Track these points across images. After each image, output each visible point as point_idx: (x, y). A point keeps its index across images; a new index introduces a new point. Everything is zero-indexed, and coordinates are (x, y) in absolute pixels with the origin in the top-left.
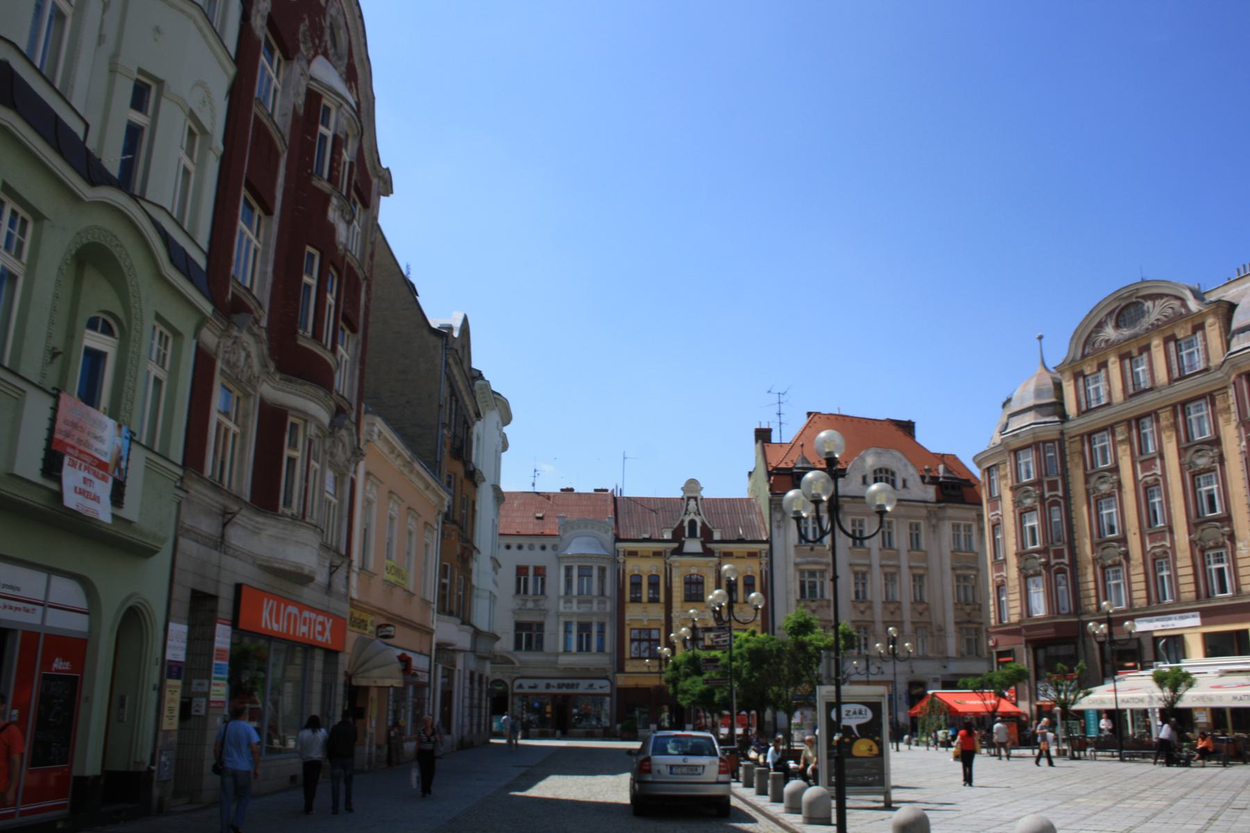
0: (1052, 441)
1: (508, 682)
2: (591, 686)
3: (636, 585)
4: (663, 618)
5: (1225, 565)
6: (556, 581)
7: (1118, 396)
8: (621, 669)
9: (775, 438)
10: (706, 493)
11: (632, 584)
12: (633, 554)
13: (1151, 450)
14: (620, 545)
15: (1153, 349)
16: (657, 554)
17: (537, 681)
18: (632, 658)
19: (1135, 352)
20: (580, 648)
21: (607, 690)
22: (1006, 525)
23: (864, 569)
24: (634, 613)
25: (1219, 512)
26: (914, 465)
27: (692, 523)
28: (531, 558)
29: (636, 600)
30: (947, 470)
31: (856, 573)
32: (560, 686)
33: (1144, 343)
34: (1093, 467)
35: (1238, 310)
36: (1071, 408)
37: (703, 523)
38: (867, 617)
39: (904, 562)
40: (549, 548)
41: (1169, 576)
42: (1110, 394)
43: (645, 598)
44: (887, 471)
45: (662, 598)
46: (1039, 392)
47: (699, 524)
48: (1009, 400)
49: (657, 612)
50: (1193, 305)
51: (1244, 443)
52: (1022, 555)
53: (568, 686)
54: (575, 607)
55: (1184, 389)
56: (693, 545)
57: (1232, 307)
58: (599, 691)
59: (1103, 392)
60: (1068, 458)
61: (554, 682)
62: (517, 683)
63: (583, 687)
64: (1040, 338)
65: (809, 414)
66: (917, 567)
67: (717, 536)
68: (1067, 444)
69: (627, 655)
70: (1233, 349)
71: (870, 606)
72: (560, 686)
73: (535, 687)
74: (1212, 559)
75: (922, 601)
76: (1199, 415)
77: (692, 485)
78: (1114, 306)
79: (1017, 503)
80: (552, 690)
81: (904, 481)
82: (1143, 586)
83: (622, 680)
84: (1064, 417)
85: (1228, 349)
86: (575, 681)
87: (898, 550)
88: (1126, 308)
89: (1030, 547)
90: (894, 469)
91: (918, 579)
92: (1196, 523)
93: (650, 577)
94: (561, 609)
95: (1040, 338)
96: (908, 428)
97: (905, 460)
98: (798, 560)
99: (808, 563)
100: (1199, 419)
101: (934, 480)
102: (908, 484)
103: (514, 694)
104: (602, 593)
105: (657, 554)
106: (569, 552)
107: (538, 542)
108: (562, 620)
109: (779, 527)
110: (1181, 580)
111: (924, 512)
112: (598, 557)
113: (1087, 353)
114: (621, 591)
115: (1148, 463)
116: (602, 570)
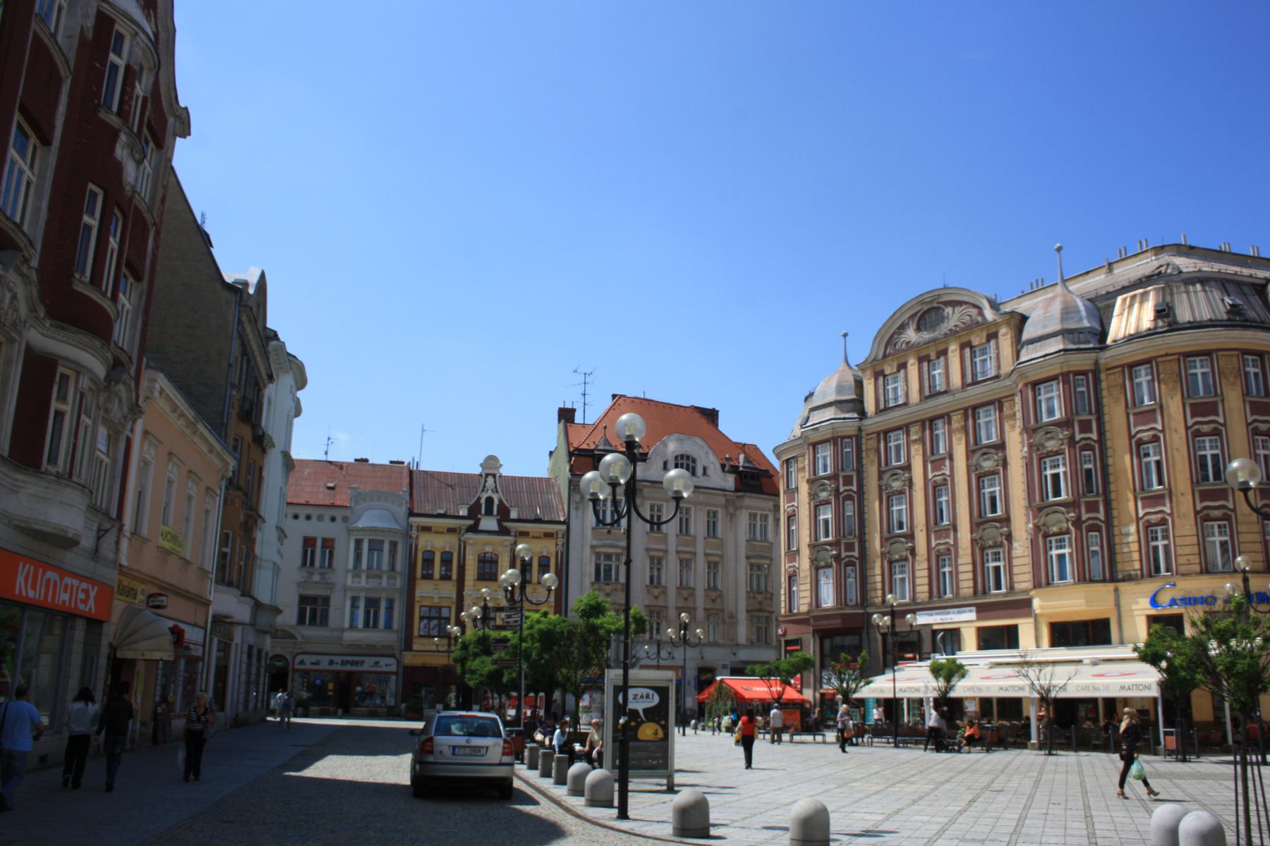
0: (850, 437)
1: (289, 657)
2: (377, 663)
3: (428, 562)
4: (454, 596)
5: (1001, 564)
6: (345, 554)
7: (915, 396)
8: (408, 646)
9: (578, 419)
10: (505, 471)
11: (424, 560)
12: (427, 529)
13: (942, 451)
14: (413, 519)
15: (950, 354)
16: (451, 530)
17: (320, 658)
18: (420, 636)
19: (933, 356)
20: (367, 625)
21: (393, 668)
22: (801, 515)
23: (660, 554)
24: (424, 590)
25: (999, 513)
27: (490, 501)
28: (319, 530)
29: (428, 577)
30: (747, 460)
31: (652, 558)
32: (344, 663)
33: (942, 347)
34: (887, 464)
35: (1029, 322)
36: (870, 406)
37: (500, 501)
38: (661, 602)
39: (700, 549)
40: (339, 519)
41: (951, 572)
42: (907, 394)
43: (437, 575)
44: (688, 457)
45: (454, 576)
46: (840, 388)
47: (496, 502)
48: (811, 395)
49: (449, 590)
50: (989, 315)
51: (1026, 449)
52: (815, 547)
53: (352, 663)
54: (363, 582)
55: (976, 394)
56: (489, 523)
57: (1023, 319)
58: (385, 669)
59: (900, 392)
60: (864, 454)
61: (338, 659)
62: (298, 659)
63: (368, 664)
64: (845, 335)
65: (614, 396)
67: (514, 515)
68: (864, 441)
69: (416, 633)
70: (1022, 359)
71: (664, 592)
72: (344, 663)
73: (317, 663)
75: (715, 588)
76: (988, 418)
77: (491, 462)
78: (912, 312)
79: (813, 496)
80: (335, 667)
81: (705, 469)
82: (926, 580)
83: (409, 659)
84: (863, 414)
86: (360, 659)
87: (695, 537)
88: (928, 312)
89: (823, 540)
90: (696, 456)
91: (713, 566)
92: (978, 523)
93: (443, 553)
94: (349, 583)
95: (845, 335)
96: (711, 416)
97: (706, 447)
98: (595, 543)
99: (604, 546)
100: (988, 423)
101: (734, 470)
102: (709, 472)
103: (295, 671)
104: (393, 567)
105: (451, 530)
106: (360, 525)
107: (328, 513)
108: (349, 594)
109: (577, 508)
110: (961, 577)
111: (723, 500)
112: (390, 531)
113: (888, 354)
114: (412, 567)
115: (938, 464)
116: (394, 545)
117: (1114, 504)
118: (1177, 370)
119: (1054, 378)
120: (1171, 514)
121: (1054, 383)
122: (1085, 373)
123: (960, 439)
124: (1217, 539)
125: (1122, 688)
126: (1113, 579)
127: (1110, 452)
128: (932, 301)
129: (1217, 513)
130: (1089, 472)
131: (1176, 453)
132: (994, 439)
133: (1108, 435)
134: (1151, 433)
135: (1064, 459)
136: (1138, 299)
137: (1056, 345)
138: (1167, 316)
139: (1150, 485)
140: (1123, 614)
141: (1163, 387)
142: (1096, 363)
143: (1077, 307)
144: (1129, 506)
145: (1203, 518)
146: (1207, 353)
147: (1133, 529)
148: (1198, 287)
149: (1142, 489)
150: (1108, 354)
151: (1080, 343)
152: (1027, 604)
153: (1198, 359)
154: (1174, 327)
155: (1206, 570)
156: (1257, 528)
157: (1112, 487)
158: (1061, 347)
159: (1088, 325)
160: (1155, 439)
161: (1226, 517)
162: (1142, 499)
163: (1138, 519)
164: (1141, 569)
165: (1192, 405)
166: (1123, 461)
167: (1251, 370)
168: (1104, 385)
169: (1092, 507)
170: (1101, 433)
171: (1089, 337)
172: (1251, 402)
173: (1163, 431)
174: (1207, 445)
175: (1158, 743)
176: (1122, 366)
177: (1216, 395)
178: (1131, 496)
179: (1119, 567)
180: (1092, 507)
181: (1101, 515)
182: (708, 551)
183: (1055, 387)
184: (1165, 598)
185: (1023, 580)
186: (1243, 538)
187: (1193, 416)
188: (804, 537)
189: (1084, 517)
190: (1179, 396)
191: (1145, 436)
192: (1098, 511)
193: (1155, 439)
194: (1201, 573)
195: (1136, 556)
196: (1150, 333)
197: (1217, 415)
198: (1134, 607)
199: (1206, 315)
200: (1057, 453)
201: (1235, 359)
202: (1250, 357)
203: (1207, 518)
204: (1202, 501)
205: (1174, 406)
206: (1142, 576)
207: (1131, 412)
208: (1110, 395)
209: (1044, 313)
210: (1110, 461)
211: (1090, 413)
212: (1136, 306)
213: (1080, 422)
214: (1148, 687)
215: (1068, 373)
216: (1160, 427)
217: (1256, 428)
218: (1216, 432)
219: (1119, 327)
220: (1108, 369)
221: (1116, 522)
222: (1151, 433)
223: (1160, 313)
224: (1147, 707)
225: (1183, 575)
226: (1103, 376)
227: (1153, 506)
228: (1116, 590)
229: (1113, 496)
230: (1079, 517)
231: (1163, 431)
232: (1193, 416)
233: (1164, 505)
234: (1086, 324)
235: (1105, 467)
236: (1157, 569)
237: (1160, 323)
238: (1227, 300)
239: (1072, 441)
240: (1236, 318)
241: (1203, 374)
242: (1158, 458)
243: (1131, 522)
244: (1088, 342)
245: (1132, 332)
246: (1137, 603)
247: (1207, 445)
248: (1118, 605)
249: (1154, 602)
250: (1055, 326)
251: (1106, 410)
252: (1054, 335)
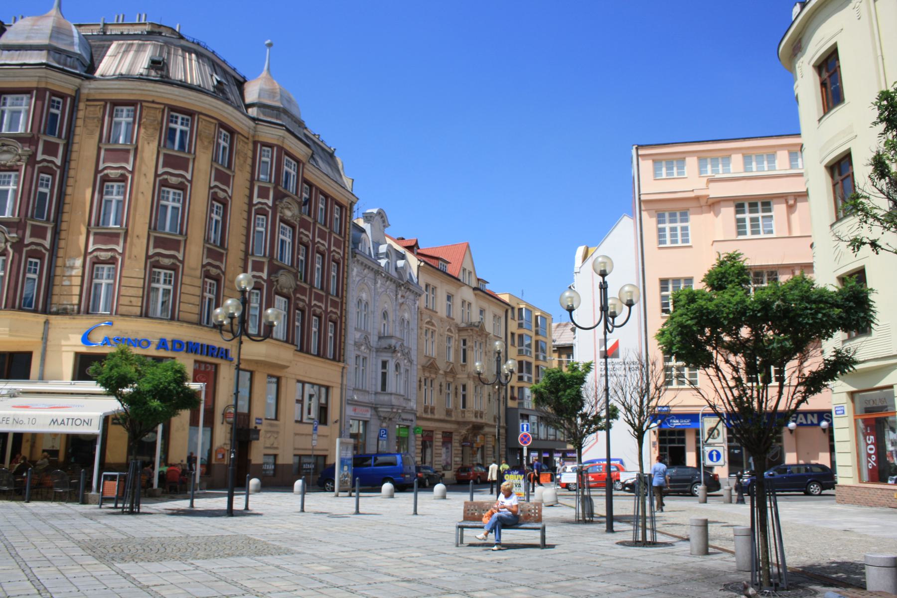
117: (63, 235)
118: (160, 119)
119: (27, 91)
120: (122, 254)
121: (25, 97)
122: (63, 96)
124: (161, 286)
125: (54, 422)
126: (45, 311)
127: (71, 182)
129: (166, 262)
130: (43, 195)
131: (140, 196)
133: (73, 164)
134: (120, 171)
135: (18, 177)
136: (135, 48)
137: (39, 58)
138: (162, 69)
139: (106, 221)
140: (49, 349)
141: (142, 130)
142: (78, 91)
143: (71, 31)
144: (79, 239)
145: (153, 264)
146: (191, 113)
147: (79, 262)
149: (97, 224)
150: (93, 84)
151: (65, 65)
153: (180, 116)
154: (166, 80)
155: (145, 314)
156: (199, 282)
157: (65, 217)
159: (79, 52)
160: (123, 179)
161: (174, 268)
162: (95, 234)
163: (86, 254)
164: (79, 305)
165: (165, 155)
166: (83, 193)
167: (223, 143)
168: (81, 114)
169: (39, 232)
170: (66, 160)
171: (77, 63)
172: (217, 169)
173: (132, 172)
174: (171, 197)
175: (89, 487)
176: (106, 101)
177: (189, 152)
178: (84, 230)
179: (55, 299)
180: (39, 232)
181: (47, 243)
183: (24, 102)
184: (98, 337)
186: (185, 289)
187: (164, 166)
189: (27, 240)
190: (156, 143)
191: (113, 173)
193: (123, 179)
194: (141, 316)
195: (76, 290)
196: (140, 78)
197: (187, 171)
198: (63, 342)
200: (11, 169)
201: (213, 126)
202: (224, 132)
203: (157, 265)
204: (155, 247)
205: (149, 151)
206: (79, 312)
207: (104, 147)
208: (85, 126)
210: (69, 190)
211: (60, 137)
212: (131, 54)
213: (46, 143)
214: (88, 422)
215: (46, 89)
217: (216, 193)
218: (181, 187)
219: (108, 66)
220: (88, 100)
221: (61, 253)
222: (120, 171)
223: (155, 64)
224: (57, 447)
225: (122, 315)
226: (82, 106)
227: (105, 243)
228: (47, 322)
229: (64, 226)
230: (22, 239)
231: (132, 172)
232: (164, 166)
233: (118, 244)
234: (77, 49)
235: (62, 195)
236: (96, 307)
237: (153, 73)
239: (32, 160)
241: (182, 132)
242: (121, 198)
243: (79, 256)
244: (76, 68)
245: (124, 72)
246: (68, 339)
247: (171, 197)
248: (45, 338)
249: (86, 340)
250: (45, 41)
251: (77, 139)
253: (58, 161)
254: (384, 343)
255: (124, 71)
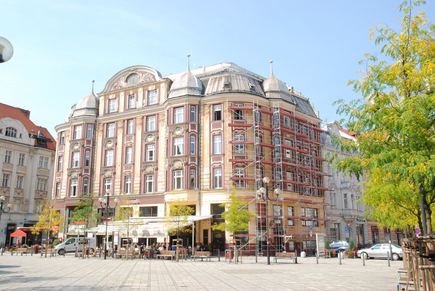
0: (91, 124)
5: (152, 181)
7: (122, 110)
13: (131, 132)
15: (139, 93)
22: (67, 156)
25: (153, 160)
26: (27, 128)
30: (41, 133)
34: (106, 137)
36: (101, 112)
39: (15, 170)
41: (130, 184)
42: (118, 109)
44: (13, 129)
46: (89, 102)
48: (75, 105)
50: (158, 79)
51: (168, 134)
52: (71, 171)
55: (149, 111)
57: (171, 82)
59: (116, 107)
64: (93, 81)
66: (20, 173)
70: (169, 97)
74: (148, 178)
75: (20, 188)
76: (152, 121)
79: (72, 147)
81: (21, 135)
84: (98, 114)
85: (168, 97)
88: (131, 74)
89: (74, 167)
90: (17, 129)
91: (20, 178)
92: (144, 164)
95: (93, 81)
96: (27, 113)
97: (22, 125)
100: (151, 123)
101: (35, 137)
102: (22, 136)
110: (135, 185)
113: (112, 89)
115: (129, 139)
120: (224, 164)
122: (195, 105)
123: (140, 128)
128: (133, 70)
132: (154, 129)
133: (202, 131)
136: (218, 79)
137: (184, 92)
148: (240, 77)
150: (205, 99)
152: (163, 196)
158: (187, 94)
159: (198, 87)
170: (199, 130)
182: (18, 171)
185: (161, 188)
188: (66, 165)
191: (216, 133)
192: (195, 161)
199: (243, 88)
209: (180, 81)
212: (217, 82)
216: (222, 129)
219: (209, 90)
226: (202, 108)
228: (199, 193)
231: (223, 131)
237: (226, 89)
238: (250, 84)
240: (252, 92)
248: (200, 199)
252: (184, 88)
253: (196, 131)
254: (344, 185)
255: (215, 90)
